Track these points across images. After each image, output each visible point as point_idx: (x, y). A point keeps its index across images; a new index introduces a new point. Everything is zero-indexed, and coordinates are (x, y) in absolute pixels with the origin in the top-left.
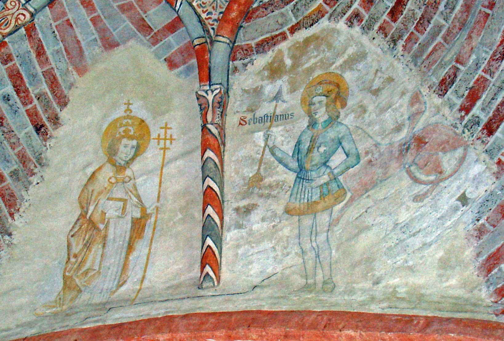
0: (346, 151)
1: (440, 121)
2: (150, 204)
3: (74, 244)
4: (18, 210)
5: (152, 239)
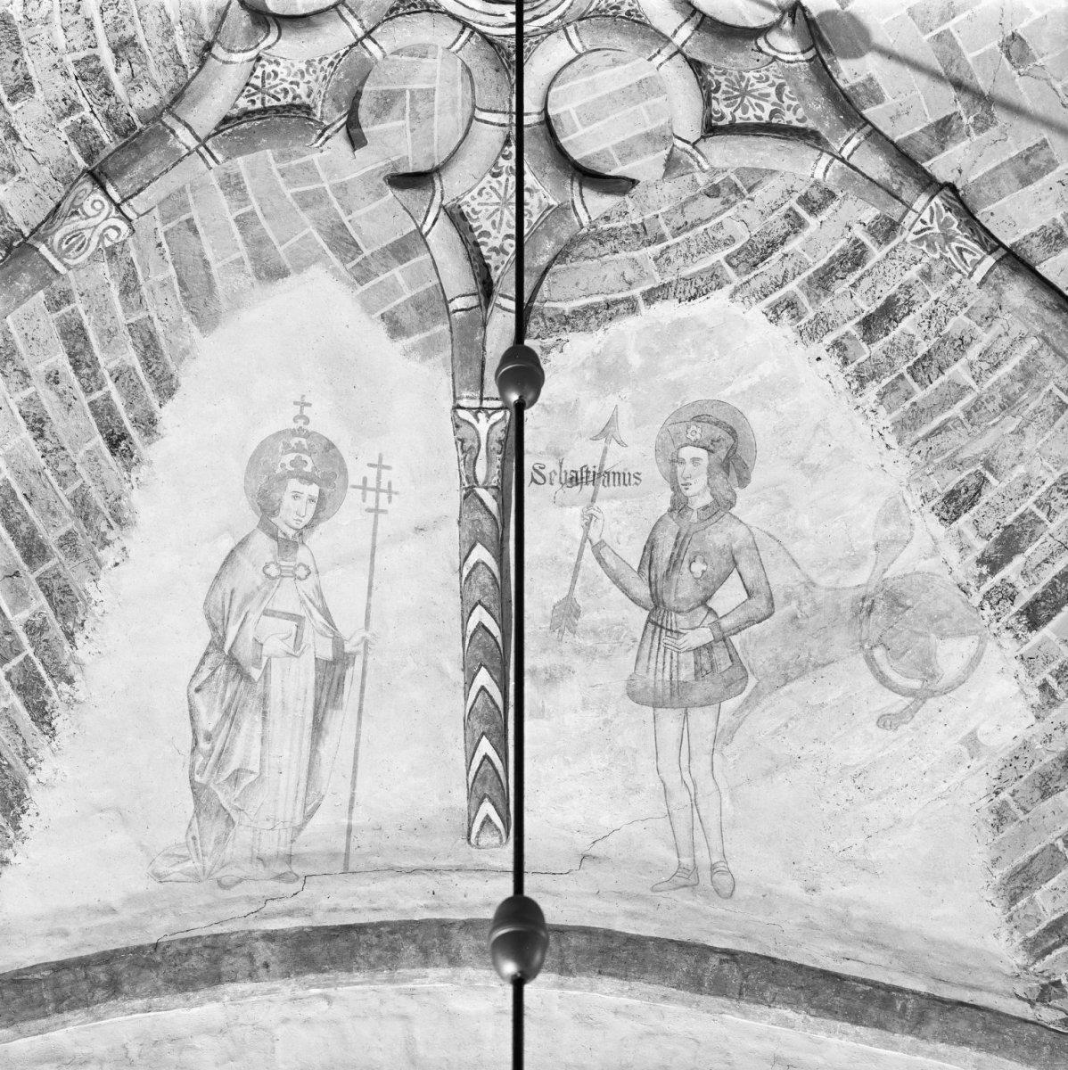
0: (748, 584)
1: (937, 571)
2: (350, 628)
3: (202, 709)
4: (82, 625)
5: (360, 710)
